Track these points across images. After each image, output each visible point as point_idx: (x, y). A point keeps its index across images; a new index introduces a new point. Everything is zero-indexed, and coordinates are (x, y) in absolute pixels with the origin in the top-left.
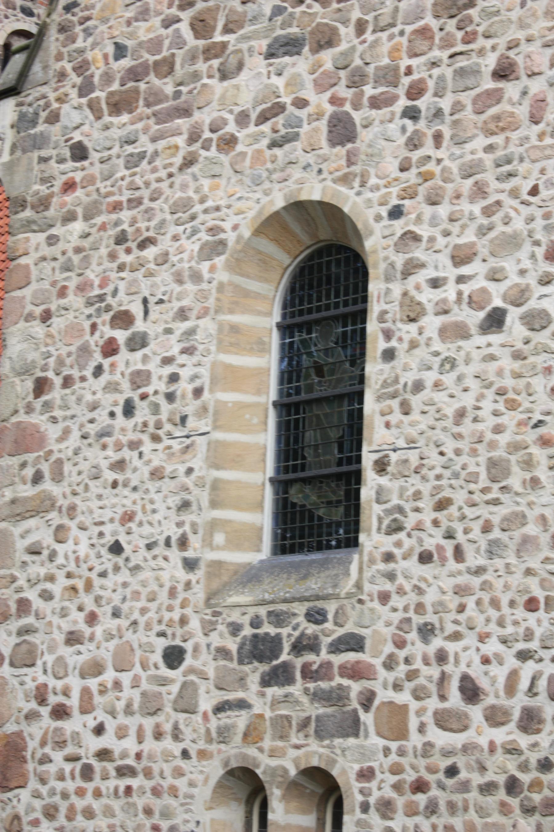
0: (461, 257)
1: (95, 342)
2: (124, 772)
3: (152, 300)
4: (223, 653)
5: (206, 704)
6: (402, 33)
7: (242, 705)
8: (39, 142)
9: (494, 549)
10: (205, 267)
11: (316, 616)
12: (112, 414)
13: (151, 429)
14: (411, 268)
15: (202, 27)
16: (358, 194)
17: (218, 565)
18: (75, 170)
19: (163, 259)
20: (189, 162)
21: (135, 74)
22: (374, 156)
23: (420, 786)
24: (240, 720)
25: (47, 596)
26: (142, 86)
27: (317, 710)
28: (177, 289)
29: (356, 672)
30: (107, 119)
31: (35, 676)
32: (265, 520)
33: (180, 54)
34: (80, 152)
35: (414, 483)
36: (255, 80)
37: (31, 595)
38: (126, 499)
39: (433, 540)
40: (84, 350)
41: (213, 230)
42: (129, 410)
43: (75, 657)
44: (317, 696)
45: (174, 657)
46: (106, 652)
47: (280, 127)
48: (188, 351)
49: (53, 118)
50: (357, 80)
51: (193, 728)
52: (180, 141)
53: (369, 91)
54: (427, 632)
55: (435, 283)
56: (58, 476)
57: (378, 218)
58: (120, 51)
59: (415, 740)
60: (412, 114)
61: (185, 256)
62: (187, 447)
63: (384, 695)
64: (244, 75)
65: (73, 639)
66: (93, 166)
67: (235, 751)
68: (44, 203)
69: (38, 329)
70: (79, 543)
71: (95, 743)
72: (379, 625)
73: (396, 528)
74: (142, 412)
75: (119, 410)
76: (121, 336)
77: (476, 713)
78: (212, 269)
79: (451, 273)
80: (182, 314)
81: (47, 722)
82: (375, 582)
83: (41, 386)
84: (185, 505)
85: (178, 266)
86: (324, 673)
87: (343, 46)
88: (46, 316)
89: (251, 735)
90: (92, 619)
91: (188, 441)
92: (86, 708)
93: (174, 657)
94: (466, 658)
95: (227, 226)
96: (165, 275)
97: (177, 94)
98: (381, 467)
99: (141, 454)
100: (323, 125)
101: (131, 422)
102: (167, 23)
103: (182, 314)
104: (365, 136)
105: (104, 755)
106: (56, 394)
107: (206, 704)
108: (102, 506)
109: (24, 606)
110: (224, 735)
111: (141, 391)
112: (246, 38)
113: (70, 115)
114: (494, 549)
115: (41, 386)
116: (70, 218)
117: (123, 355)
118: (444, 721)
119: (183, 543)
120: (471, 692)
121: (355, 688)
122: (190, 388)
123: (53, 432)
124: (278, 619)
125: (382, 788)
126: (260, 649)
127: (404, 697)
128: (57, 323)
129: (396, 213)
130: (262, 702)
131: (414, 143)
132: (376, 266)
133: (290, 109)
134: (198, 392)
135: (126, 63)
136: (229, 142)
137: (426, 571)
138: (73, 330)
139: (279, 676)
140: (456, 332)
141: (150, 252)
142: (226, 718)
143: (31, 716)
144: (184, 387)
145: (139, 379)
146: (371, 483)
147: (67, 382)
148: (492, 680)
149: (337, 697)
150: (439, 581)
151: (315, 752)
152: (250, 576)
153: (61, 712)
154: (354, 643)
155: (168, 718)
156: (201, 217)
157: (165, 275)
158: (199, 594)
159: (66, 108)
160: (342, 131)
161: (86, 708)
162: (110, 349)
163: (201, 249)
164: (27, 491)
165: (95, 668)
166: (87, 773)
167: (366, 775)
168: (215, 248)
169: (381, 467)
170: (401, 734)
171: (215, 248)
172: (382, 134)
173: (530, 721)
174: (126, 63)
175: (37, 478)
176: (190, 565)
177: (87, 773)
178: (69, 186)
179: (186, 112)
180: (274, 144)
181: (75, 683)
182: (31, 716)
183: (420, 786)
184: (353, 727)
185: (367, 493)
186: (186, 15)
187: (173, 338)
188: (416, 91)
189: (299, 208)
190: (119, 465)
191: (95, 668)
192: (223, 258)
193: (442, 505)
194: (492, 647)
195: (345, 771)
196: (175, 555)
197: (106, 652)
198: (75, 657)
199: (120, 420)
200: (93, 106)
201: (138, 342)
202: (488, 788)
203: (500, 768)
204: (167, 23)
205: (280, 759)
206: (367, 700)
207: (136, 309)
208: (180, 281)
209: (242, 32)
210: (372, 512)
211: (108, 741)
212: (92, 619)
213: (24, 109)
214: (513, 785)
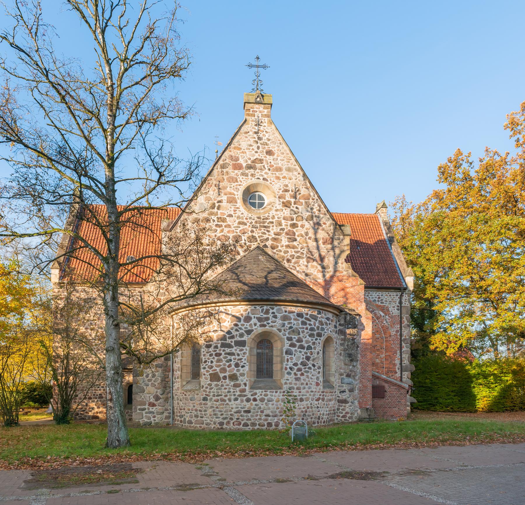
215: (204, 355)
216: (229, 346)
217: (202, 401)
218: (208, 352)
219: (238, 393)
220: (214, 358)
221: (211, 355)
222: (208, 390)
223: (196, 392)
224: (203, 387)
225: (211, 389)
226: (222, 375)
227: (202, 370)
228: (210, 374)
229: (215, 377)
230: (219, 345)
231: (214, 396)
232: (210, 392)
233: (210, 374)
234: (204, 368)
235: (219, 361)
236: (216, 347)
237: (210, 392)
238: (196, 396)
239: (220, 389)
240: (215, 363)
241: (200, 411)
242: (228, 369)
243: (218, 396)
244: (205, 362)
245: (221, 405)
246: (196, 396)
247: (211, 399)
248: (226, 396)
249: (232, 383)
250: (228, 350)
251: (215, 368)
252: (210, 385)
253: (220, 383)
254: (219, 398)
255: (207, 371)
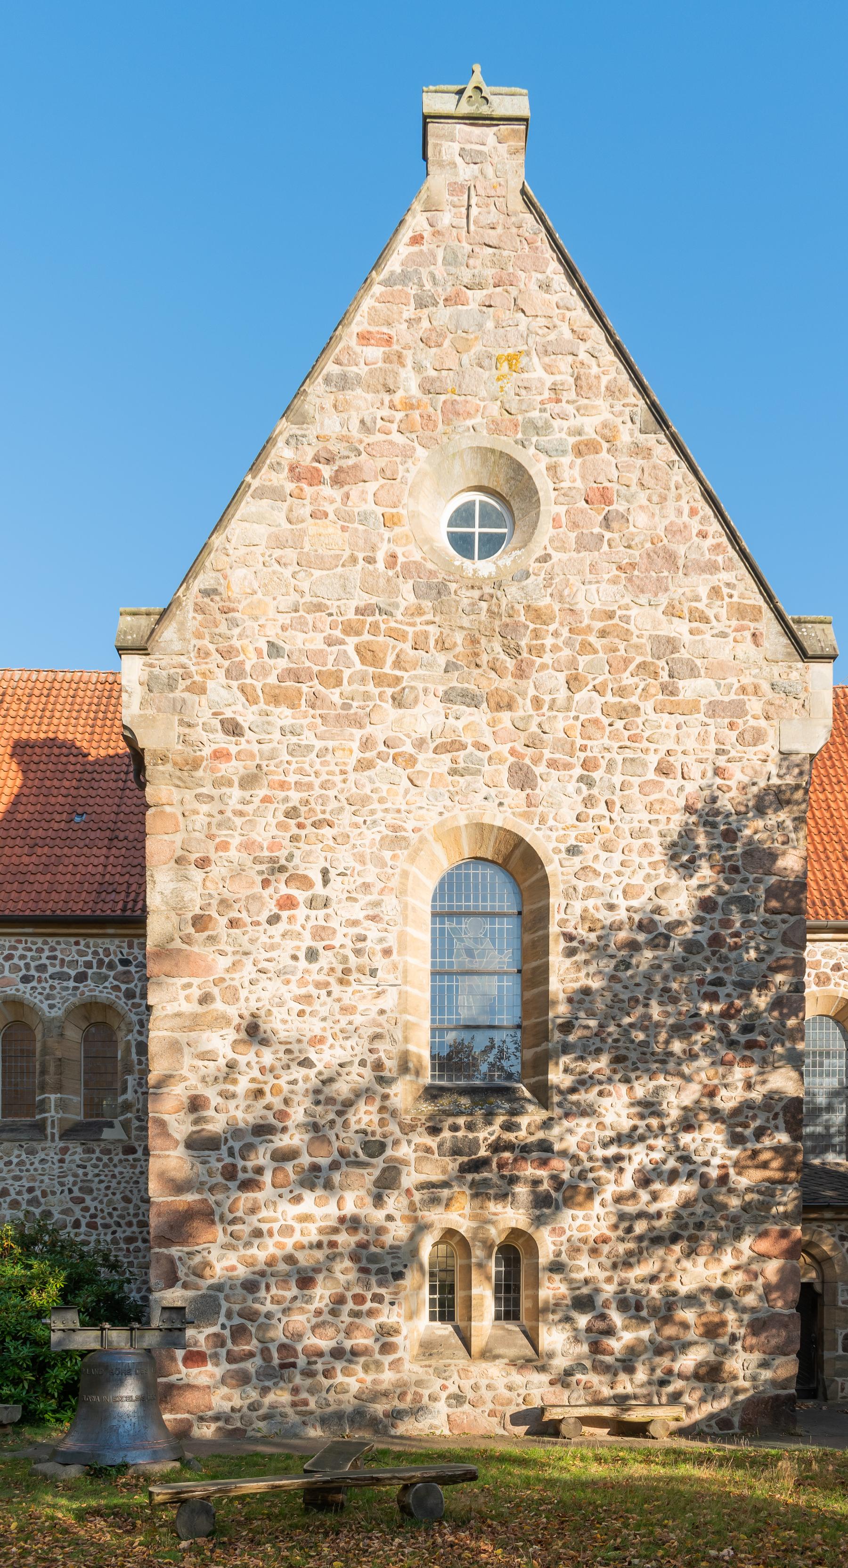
3: (332, 874)
6: (576, 718)
10: (387, 854)
12: (295, 958)
13: (339, 974)
16: (538, 829)
18: (230, 743)
26: (304, 688)
28: (358, 867)
30: (262, 705)
33: (347, 673)
34: (233, 729)
41: (395, 829)
42: (312, 955)
47: (460, 760)
48: (373, 918)
52: (355, 745)
57: (556, 851)
58: (274, 650)
61: (367, 842)
62: (379, 994)
66: (247, 743)
75: (302, 955)
78: (394, 857)
85: (360, 849)
87: (520, 713)
91: (379, 989)
95: (409, 826)
97: (346, 706)
99: (329, 994)
100: (504, 770)
101: (315, 967)
104: (543, 789)
111: (324, 943)
112: (415, 678)
122: (379, 947)
129: (573, 851)
132: (555, 886)
133: (470, 749)
134: (387, 952)
135: (282, 663)
156: (379, 815)
159: (210, 685)
163: (382, 839)
174: (282, 663)
180: (453, 772)
186: (352, 641)
187: (357, 906)
192: (406, 852)
199: (303, 963)
208: (363, 863)
209: (413, 673)
213: (156, 671)
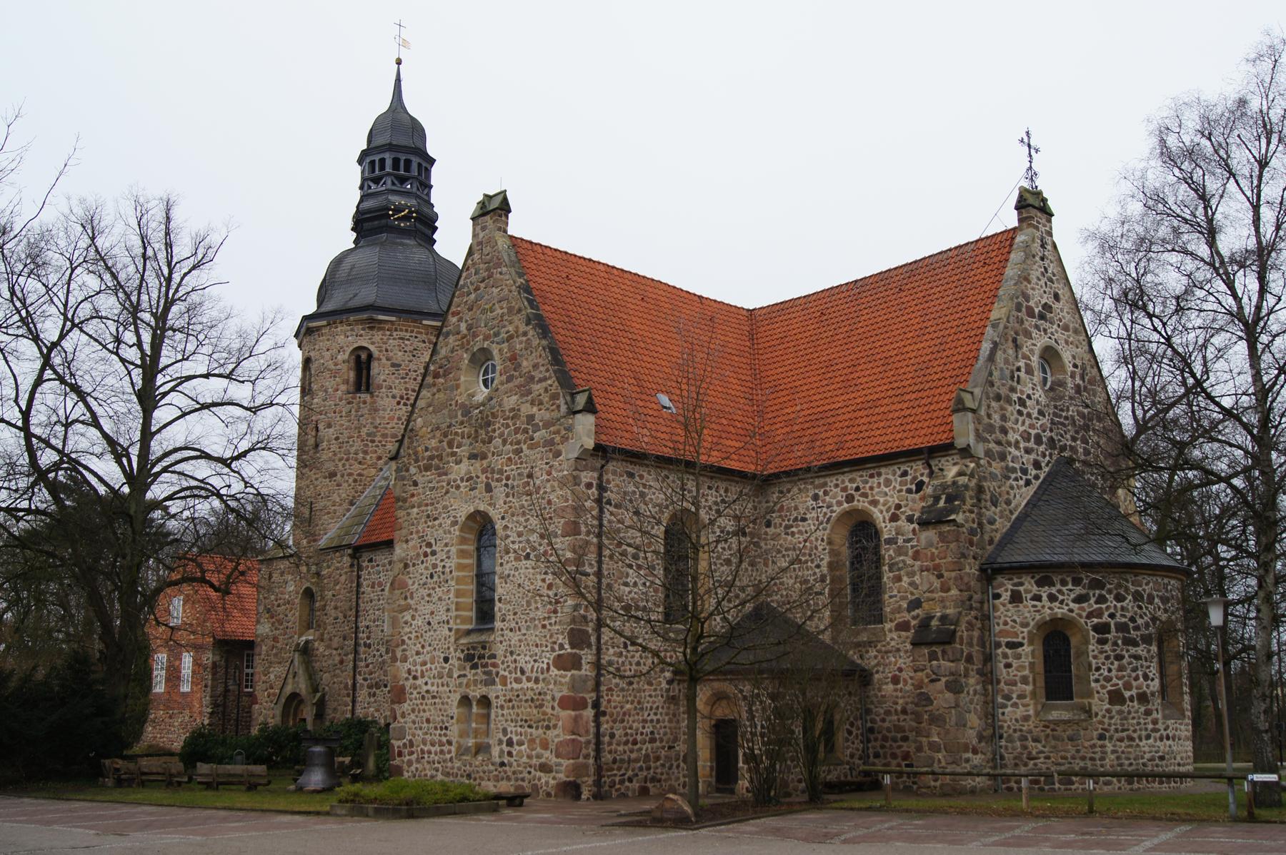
0: (520, 534)
1: (421, 551)
2: (434, 697)
4: (459, 659)
5: (455, 676)
7: (465, 676)
8: (403, 478)
9: (528, 628)
11: (484, 648)
14: (507, 537)
15: (450, 445)
17: (458, 630)
19: (440, 525)
20: (447, 492)
21: (431, 458)
22: (498, 498)
23: (510, 701)
24: (465, 681)
25: (410, 638)
27: (484, 677)
29: (494, 665)
31: (407, 665)
32: (473, 614)
34: (415, 484)
35: (508, 607)
36: (464, 468)
37: (405, 638)
38: (431, 607)
39: (513, 625)
40: (418, 555)
42: (432, 577)
43: (419, 659)
44: (485, 673)
45: (446, 660)
46: (428, 658)
49: (407, 470)
50: (493, 472)
51: (452, 683)
53: (496, 476)
54: (512, 653)
55: (513, 542)
56: (412, 598)
59: (509, 686)
60: (506, 485)
63: (502, 673)
64: (462, 465)
65: (418, 653)
67: (462, 690)
68: (405, 500)
69: (405, 546)
70: (419, 622)
71: (425, 688)
72: (500, 650)
73: (503, 620)
74: (436, 578)
76: (429, 550)
77: (524, 678)
79: (517, 539)
80: (446, 545)
81: (411, 681)
82: (504, 638)
83: (406, 566)
84: (448, 610)
86: (485, 666)
88: (407, 541)
89: (468, 685)
90: (423, 647)
92: (423, 676)
93: (446, 660)
94: (522, 660)
96: (441, 531)
98: (500, 600)
102: (441, 442)
103: (446, 545)
104: (495, 491)
105: (428, 692)
106: (411, 569)
107: (455, 676)
108: (425, 609)
109: (403, 642)
110: (460, 684)
113: (413, 470)
114: (528, 628)
115: (406, 566)
116: (413, 507)
117: (430, 557)
118: (518, 681)
119: (448, 622)
120: (523, 672)
121: (494, 670)
123: (410, 582)
124: (474, 648)
125: (501, 701)
126: (469, 658)
127: (506, 673)
128: (411, 544)
129: (503, 518)
130: (470, 674)
131: (507, 495)
135: (428, 453)
136: (458, 487)
137: (511, 634)
138: (414, 547)
139: (474, 667)
140: (518, 559)
141: (437, 522)
142: (462, 680)
143: (407, 679)
144: (447, 570)
145: (435, 566)
146: (498, 605)
147: (414, 565)
148: (528, 668)
149: (488, 673)
150: (515, 638)
151: (483, 690)
152: (469, 632)
153: (415, 678)
154: (494, 656)
155: (445, 679)
157: (441, 531)
158: (452, 639)
160: (489, 489)
161: (423, 676)
162: (426, 555)
164: (403, 602)
165: (424, 663)
166: (423, 697)
167: (497, 697)
168: (455, 523)
169: (500, 600)
170: (505, 685)
171: (455, 523)
172: (500, 491)
173: (537, 681)
174: (428, 453)
175: (406, 598)
176: (450, 630)
177: (423, 697)
178: (413, 495)
179: (446, 474)
181: (419, 668)
182: (407, 679)
183: (510, 701)
184: (493, 683)
185: (496, 609)
188: (508, 479)
189: (478, 512)
190: (429, 595)
191: (424, 663)
193: (515, 614)
194: (527, 658)
195: (492, 696)
196: (446, 626)
197: (428, 658)
198: (419, 659)
200: (419, 467)
201: (434, 553)
202: (526, 701)
203: (530, 694)
204: (441, 442)
205: (475, 693)
206: (497, 673)
207: (433, 541)
210: (498, 615)
211: (429, 687)
212: (423, 647)
214: (532, 700)
215: (1095, 657)
216: (1135, 644)
217: (1095, 741)
218: (1101, 652)
219: (1150, 726)
220: (1112, 663)
221: (1107, 658)
222: (1106, 720)
223: (1084, 724)
224: (1097, 714)
225: (1111, 718)
226: (1127, 694)
227: (1093, 685)
228: (1109, 692)
229: (1116, 697)
230: (1120, 642)
231: (1116, 730)
232: (1110, 725)
233: (1109, 692)
234: (1097, 681)
235: (1121, 669)
236: (1115, 644)
237: (1110, 725)
238: (1082, 733)
239: (1126, 719)
240: (1114, 673)
241: (1092, 759)
242: (1134, 684)
243: (1123, 731)
244: (1098, 669)
245: (1128, 747)
246: (1082, 733)
247: (1111, 738)
248: (1135, 731)
249: (1143, 709)
250: (1133, 650)
251: (1115, 681)
252: (1108, 711)
253: (1125, 708)
254: (1125, 734)
255: (1103, 687)
